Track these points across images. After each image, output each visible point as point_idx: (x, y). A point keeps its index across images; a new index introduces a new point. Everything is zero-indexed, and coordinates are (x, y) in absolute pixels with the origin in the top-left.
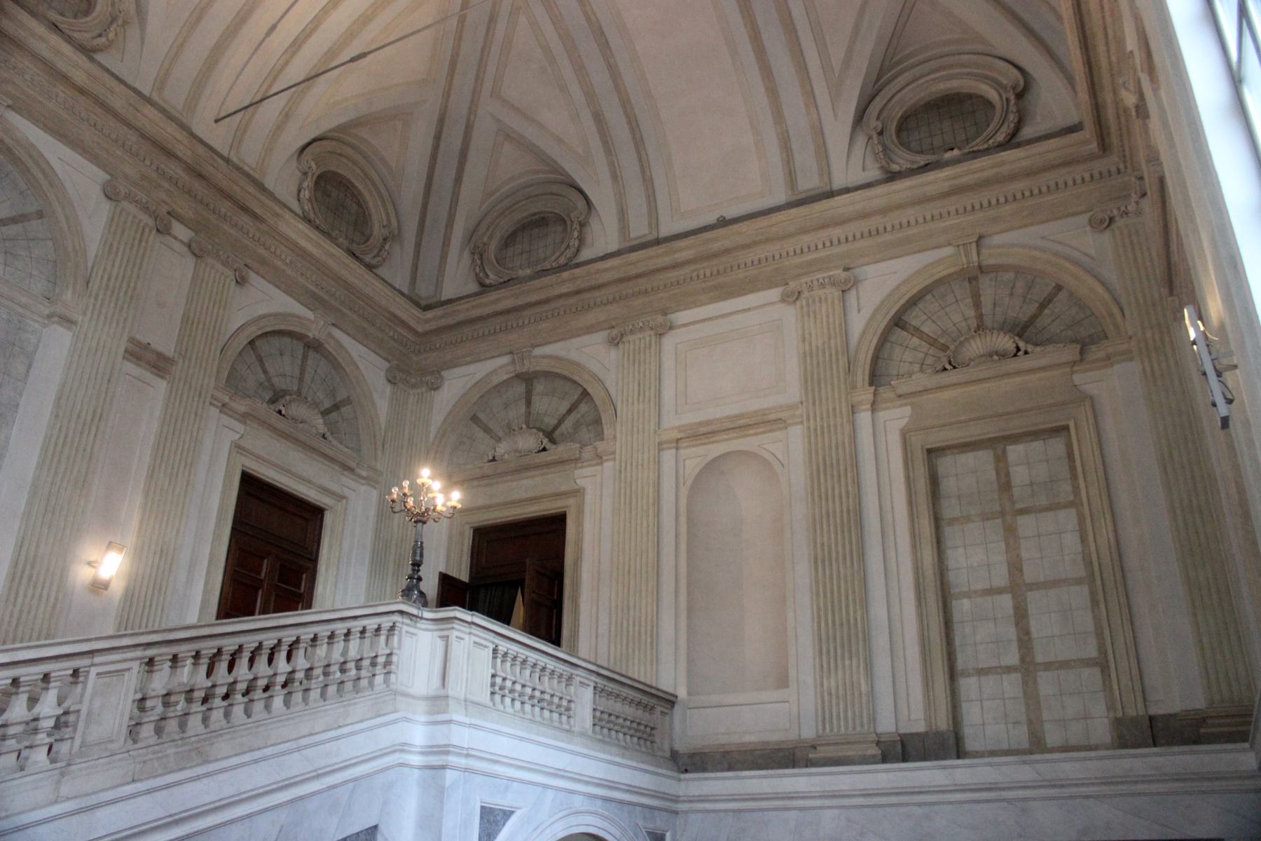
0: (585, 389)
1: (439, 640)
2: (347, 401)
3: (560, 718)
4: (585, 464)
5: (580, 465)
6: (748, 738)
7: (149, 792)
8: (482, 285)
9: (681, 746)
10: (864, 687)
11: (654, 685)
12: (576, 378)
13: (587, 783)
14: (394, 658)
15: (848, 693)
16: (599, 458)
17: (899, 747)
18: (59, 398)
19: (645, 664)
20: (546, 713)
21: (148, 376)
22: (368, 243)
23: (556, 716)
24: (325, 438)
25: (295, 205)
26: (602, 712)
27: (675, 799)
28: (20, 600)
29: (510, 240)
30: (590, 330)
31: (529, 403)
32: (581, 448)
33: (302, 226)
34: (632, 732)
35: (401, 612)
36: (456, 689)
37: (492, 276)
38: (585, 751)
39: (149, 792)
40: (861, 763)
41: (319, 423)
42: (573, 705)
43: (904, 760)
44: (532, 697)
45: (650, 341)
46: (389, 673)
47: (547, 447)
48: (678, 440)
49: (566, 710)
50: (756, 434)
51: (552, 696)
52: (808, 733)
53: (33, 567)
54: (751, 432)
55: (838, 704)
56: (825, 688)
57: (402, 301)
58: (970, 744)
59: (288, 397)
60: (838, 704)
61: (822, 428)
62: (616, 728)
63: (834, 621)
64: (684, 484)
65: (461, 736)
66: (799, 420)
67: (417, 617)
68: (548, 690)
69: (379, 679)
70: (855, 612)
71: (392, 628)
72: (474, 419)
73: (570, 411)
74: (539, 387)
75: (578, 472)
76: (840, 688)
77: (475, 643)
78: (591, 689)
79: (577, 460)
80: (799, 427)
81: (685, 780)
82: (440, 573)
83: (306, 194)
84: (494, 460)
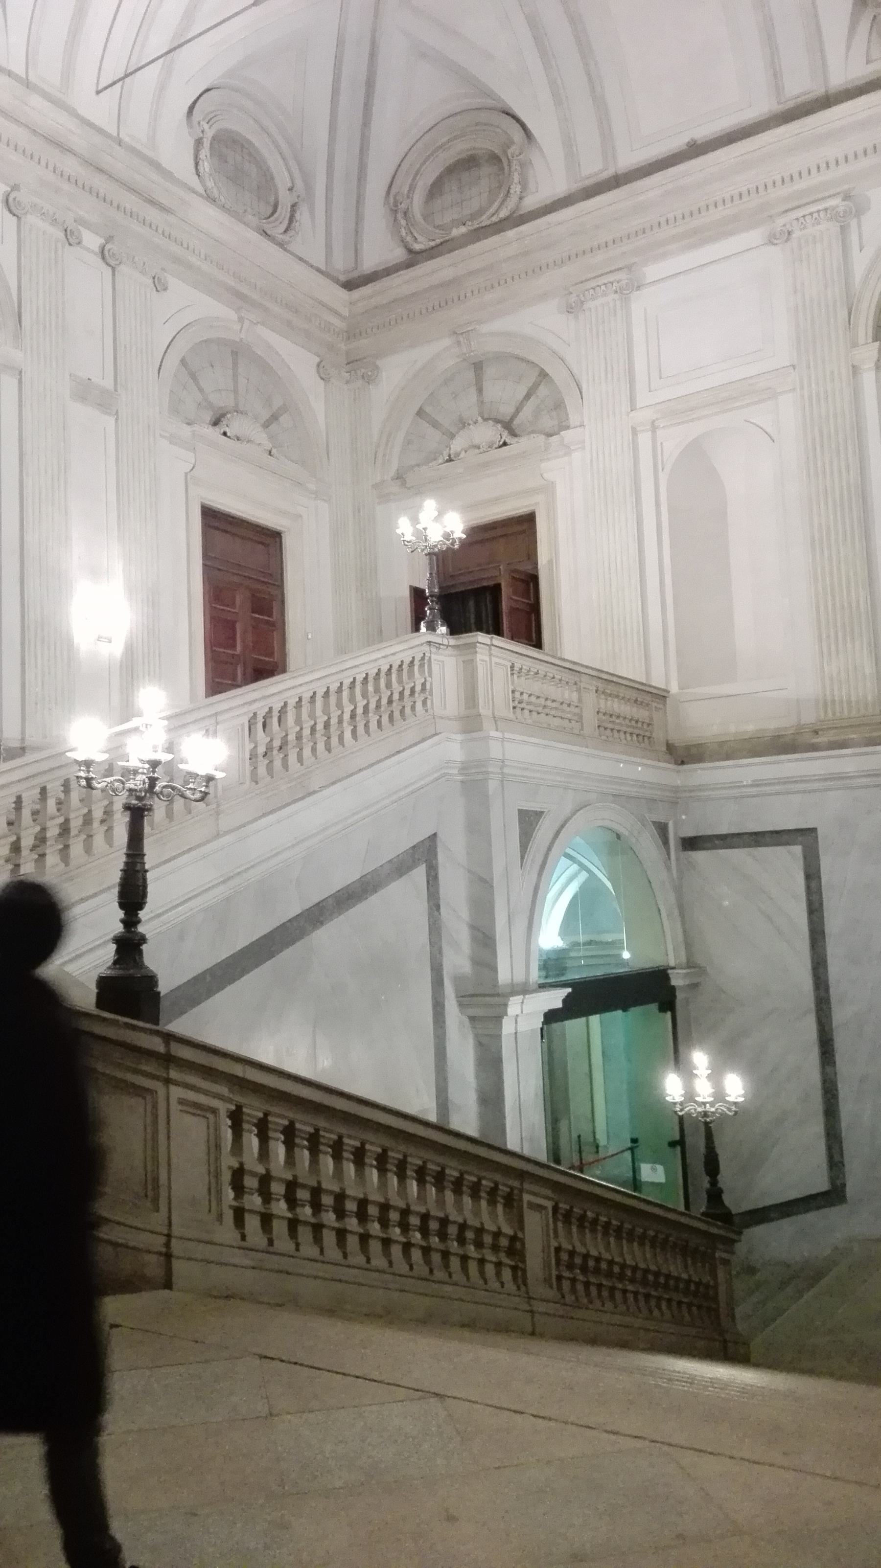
0: (543, 369)
2: (284, 409)
8: (410, 251)
9: (678, 738)
12: (531, 358)
22: (276, 215)
25: (194, 182)
28: (39, 662)
29: (435, 190)
30: (543, 297)
31: (480, 391)
33: (212, 212)
37: (420, 238)
38: (596, 752)
41: (261, 436)
45: (615, 306)
47: (508, 441)
57: (322, 280)
61: (818, 395)
69: (419, 706)
73: (528, 396)
74: (490, 372)
82: (411, 587)
83: (206, 166)
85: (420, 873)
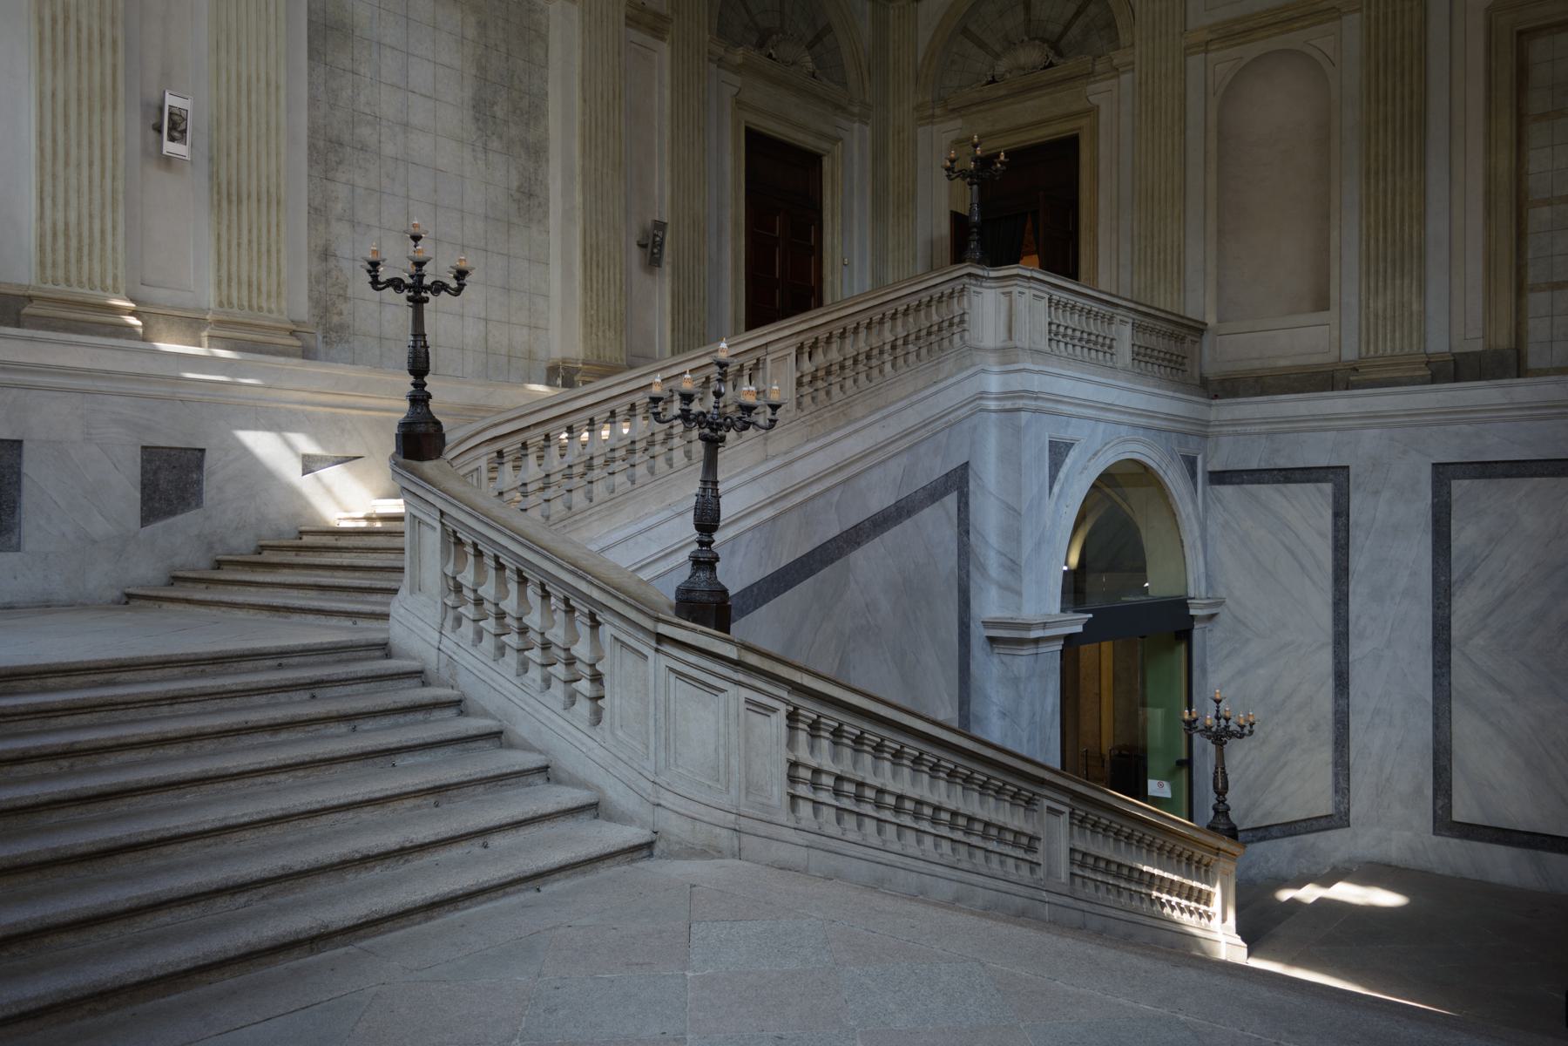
1: (1002, 296)
3: (1104, 356)
4: (1098, 78)
5: (1092, 79)
6: (1282, 363)
7: (821, 448)
9: (1212, 369)
10: (1415, 307)
11: (1182, 314)
13: (1131, 414)
14: (966, 317)
15: (1397, 314)
16: (1116, 71)
17: (1452, 366)
18: (583, 80)
19: (1172, 294)
20: (1093, 352)
21: (650, 41)
23: (1101, 354)
24: (815, 78)
26: (1140, 347)
27: (1207, 424)
32: (1094, 60)
34: (1166, 363)
35: (969, 275)
36: (1022, 339)
38: (1130, 386)
39: (821, 448)
40: (1406, 385)
42: (1115, 343)
43: (1456, 379)
44: (1081, 339)
46: (964, 330)
47: (1054, 61)
48: (1207, 43)
49: (1106, 346)
50: (1303, 28)
51: (1097, 336)
52: (1350, 354)
53: (598, 255)
54: (1296, 25)
55: (1385, 327)
56: (1372, 309)
58: (1532, 362)
59: (774, 37)
60: (1385, 327)
62: (1151, 361)
63: (1385, 239)
64: (1214, 94)
65: (1035, 383)
66: (1358, 7)
67: (983, 277)
68: (1094, 332)
69: (956, 338)
70: (1411, 227)
71: (962, 290)
72: (965, 31)
75: (1091, 88)
76: (1389, 310)
77: (1034, 295)
78: (1129, 327)
79: (1091, 74)
80: (1357, 15)
81: (1217, 405)
84: (993, 81)
85: (951, 500)
